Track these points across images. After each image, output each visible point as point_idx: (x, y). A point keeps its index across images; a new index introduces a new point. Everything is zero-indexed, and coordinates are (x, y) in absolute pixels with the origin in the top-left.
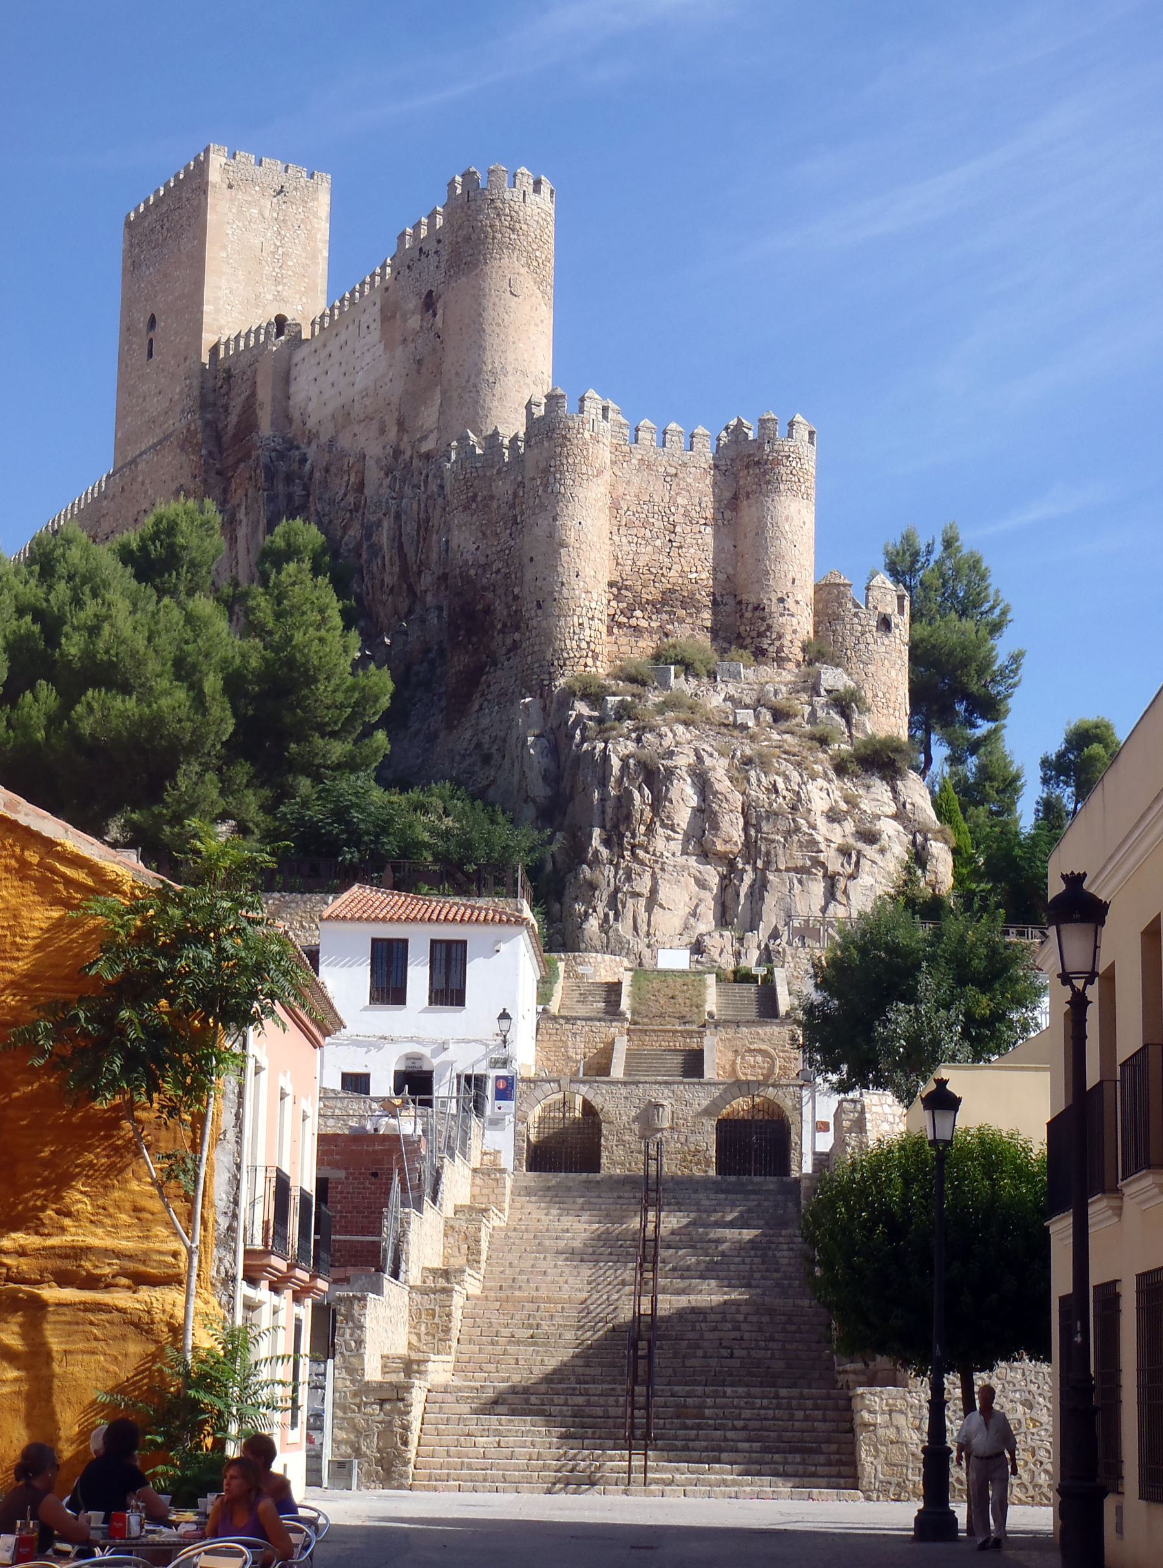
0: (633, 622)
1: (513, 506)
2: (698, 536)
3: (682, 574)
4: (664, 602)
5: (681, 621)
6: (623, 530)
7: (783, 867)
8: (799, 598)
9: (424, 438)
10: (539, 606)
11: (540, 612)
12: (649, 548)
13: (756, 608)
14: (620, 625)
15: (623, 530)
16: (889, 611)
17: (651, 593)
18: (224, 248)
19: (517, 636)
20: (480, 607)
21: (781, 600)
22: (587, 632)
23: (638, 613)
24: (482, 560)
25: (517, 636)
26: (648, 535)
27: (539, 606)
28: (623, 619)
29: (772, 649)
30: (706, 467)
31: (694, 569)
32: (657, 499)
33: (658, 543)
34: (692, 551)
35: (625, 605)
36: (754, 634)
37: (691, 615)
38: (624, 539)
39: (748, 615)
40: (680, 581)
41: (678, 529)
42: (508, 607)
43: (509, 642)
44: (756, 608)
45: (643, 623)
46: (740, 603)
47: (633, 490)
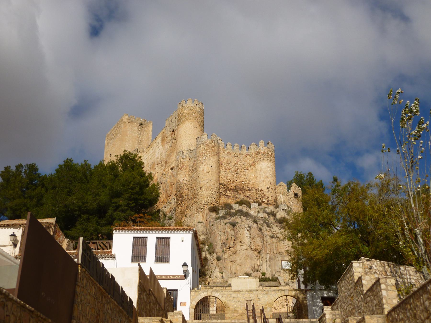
0: (227, 194)
1: (193, 167)
3: (240, 182)
4: (235, 189)
5: (240, 194)
6: (224, 170)
7: (275, 252)
8: (273, 188)
9: (172, 164)
10: (201, 189)
11: (201, 190)
12: (231, 175)
13: (261, 191)
14: (223, 195)
16: (297, 192)
17: (232, 186)
18: (127, 136)
19: (195, 200)
20: (184, 194)
21: (268, 188)
22: (214, 196)
23: (228, 192)
24: (185, 182)
25: (195, 200)
26: (230, 172)
27: (201, 189)
28: (224, 193)
29: (266, 201)
32: (232, 162)
33: (233, 174)
34: (242, 176)
36: (261, 197)
37: (243, 193)
38: (224, 173)
39: (259, 192)
41: (238, 170)
42: (192, 193)
43: (192, 202)
44: (261, 191)
45: (229, 195)
46: (256, 190)
47: (226, 160)
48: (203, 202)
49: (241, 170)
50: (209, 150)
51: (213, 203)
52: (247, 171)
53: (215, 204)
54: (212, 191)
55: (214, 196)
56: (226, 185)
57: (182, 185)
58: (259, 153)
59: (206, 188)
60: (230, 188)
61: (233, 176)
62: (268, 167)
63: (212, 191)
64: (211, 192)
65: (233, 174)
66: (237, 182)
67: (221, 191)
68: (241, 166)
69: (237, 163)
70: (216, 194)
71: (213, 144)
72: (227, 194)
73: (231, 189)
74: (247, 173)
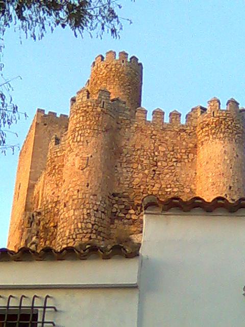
2: (173, 168)
6: (124, 165)
14: (121, 218)
15: (124, 165)
20: (52, 224)
23: (132, 211)
26: (140, 167)
28: (122, 215)
30: (177, 130)
31: (169, 186)
33: (146, 172)
34: (168, 176)
35: (123, 207)
38: (125, 170)
40: (160, 193)
41: (159, 164)
45: (134, 217)
48: (67, 235)
49: (165, 164)
50: (88, 123)
51: (88, 235)
52: (179, 165)
53: (94, 236)
54: (89, 209)
55: (93, 218)
56: (127, 197)
57: (50, 206)
58: (208, 125)
59: (76, 202)
60: (136, 202)
61: (147, 176)
62: (225, 152)
63: (89, 209)
64: (85, 211)
65: (146, 172)
66: (154, 189)
67: (114, 210)
68: (165, 155)
69: (156, 149)
70: (99, 214)
71: (99, 109)
72: (128, 216)
73: (138, 205)
74: (178, 170)
